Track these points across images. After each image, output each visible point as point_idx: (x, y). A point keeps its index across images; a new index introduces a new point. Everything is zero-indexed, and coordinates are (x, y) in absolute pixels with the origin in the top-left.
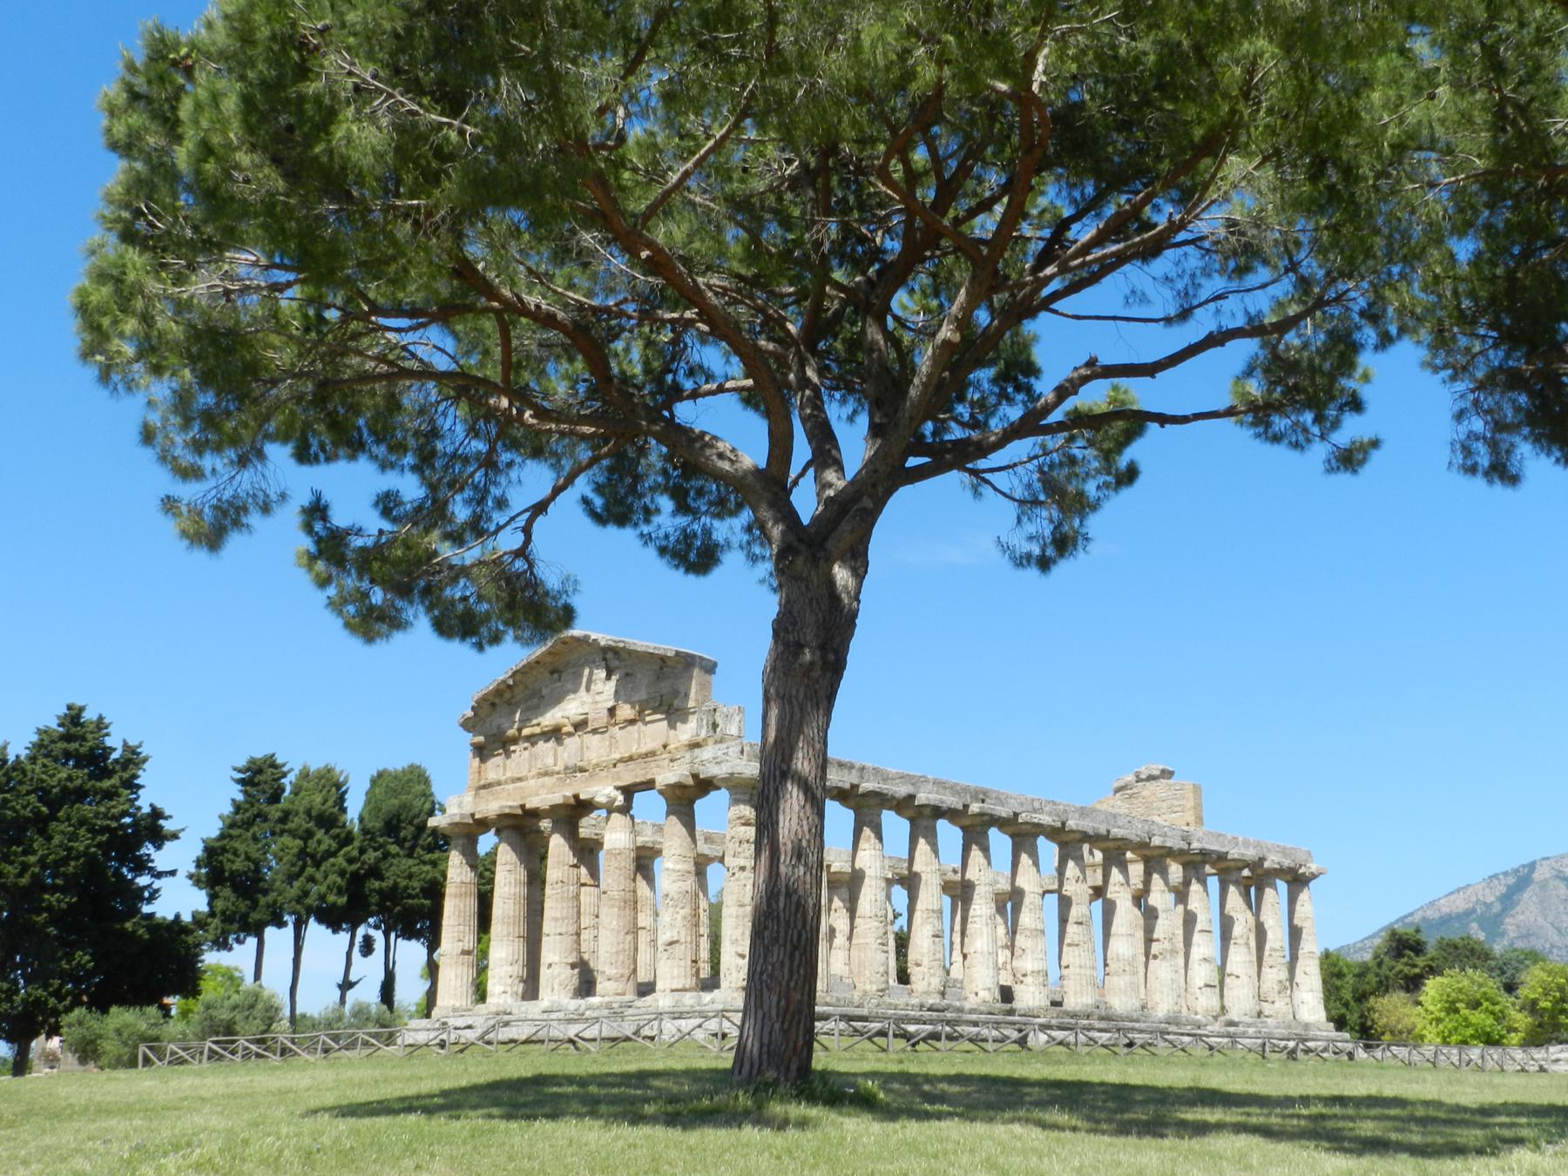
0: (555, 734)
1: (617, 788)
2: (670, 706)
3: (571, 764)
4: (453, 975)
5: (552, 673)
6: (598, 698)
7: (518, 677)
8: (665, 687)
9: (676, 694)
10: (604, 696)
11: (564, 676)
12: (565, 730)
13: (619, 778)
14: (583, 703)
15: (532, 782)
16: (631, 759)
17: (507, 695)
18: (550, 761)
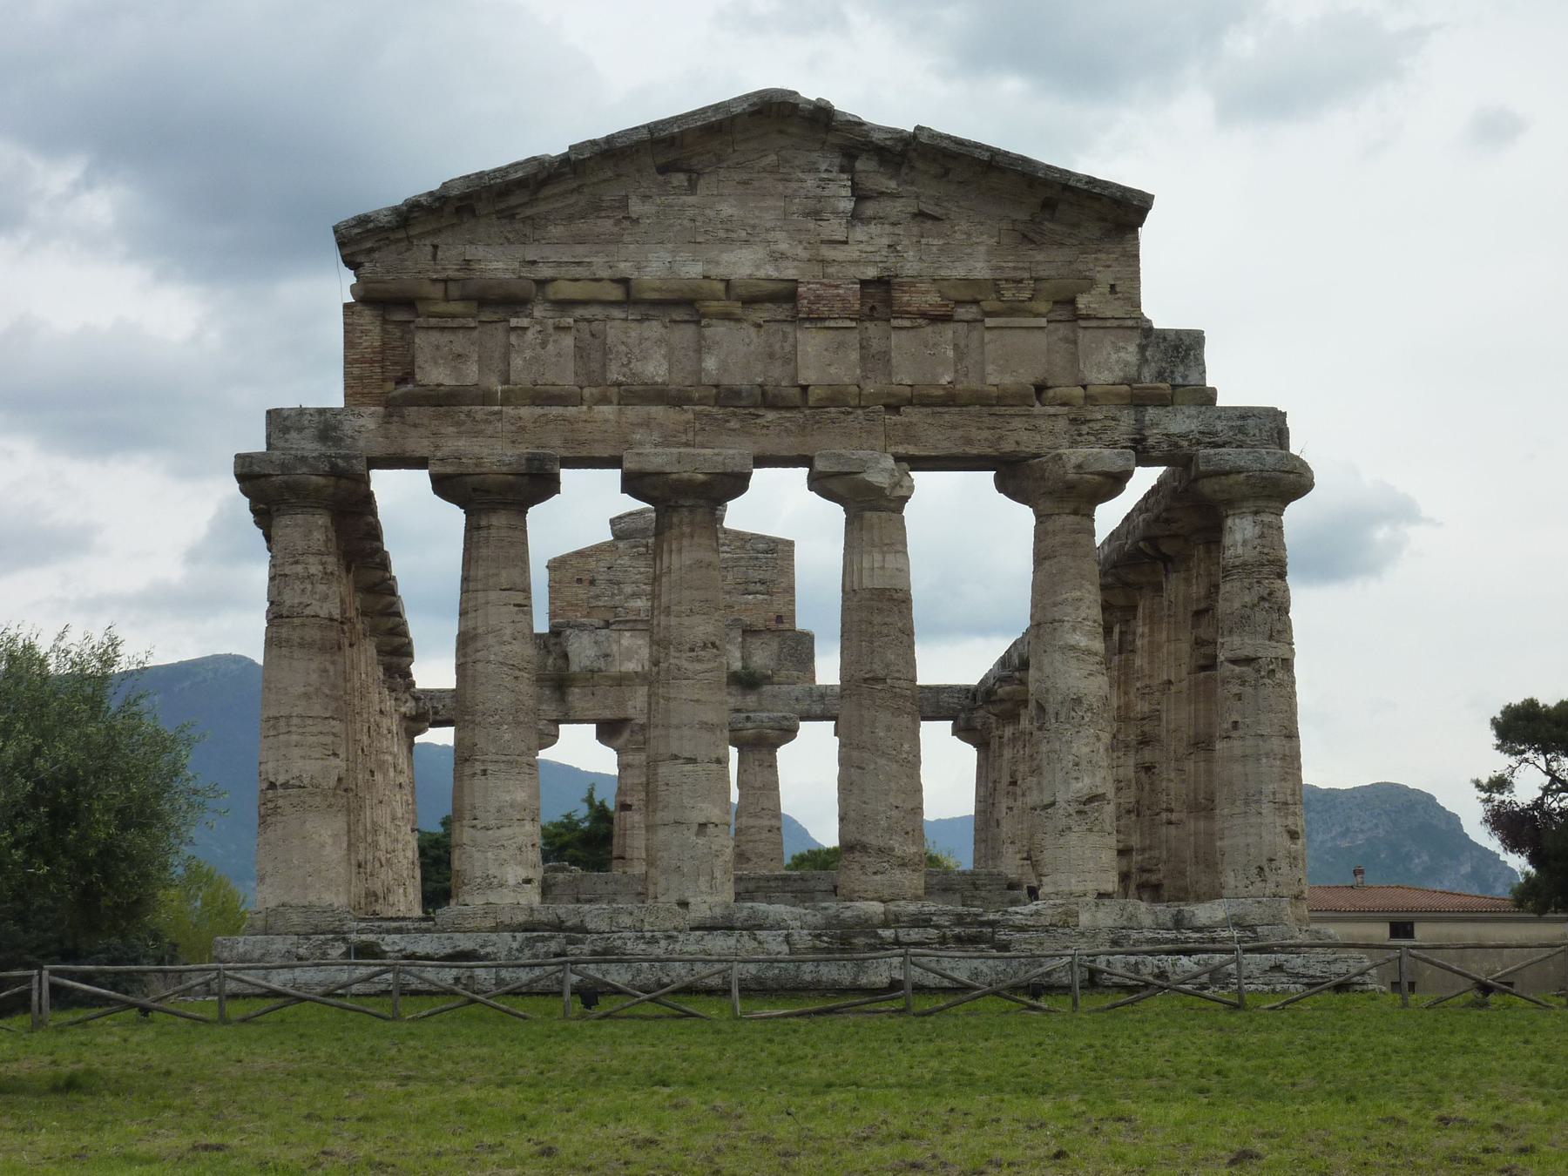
0: (685, 305)
1: (898, 459)
3: (737, 379)
4: (326, 836)
5: (664, 170)
6: (828, 252)
9: (1091, 283)
10: (852, 252)
12: (714, 306)
13: (910, 438)
14: (778, 257)
15: (607, 411)
16: (951, 399)
18: (655, 369)
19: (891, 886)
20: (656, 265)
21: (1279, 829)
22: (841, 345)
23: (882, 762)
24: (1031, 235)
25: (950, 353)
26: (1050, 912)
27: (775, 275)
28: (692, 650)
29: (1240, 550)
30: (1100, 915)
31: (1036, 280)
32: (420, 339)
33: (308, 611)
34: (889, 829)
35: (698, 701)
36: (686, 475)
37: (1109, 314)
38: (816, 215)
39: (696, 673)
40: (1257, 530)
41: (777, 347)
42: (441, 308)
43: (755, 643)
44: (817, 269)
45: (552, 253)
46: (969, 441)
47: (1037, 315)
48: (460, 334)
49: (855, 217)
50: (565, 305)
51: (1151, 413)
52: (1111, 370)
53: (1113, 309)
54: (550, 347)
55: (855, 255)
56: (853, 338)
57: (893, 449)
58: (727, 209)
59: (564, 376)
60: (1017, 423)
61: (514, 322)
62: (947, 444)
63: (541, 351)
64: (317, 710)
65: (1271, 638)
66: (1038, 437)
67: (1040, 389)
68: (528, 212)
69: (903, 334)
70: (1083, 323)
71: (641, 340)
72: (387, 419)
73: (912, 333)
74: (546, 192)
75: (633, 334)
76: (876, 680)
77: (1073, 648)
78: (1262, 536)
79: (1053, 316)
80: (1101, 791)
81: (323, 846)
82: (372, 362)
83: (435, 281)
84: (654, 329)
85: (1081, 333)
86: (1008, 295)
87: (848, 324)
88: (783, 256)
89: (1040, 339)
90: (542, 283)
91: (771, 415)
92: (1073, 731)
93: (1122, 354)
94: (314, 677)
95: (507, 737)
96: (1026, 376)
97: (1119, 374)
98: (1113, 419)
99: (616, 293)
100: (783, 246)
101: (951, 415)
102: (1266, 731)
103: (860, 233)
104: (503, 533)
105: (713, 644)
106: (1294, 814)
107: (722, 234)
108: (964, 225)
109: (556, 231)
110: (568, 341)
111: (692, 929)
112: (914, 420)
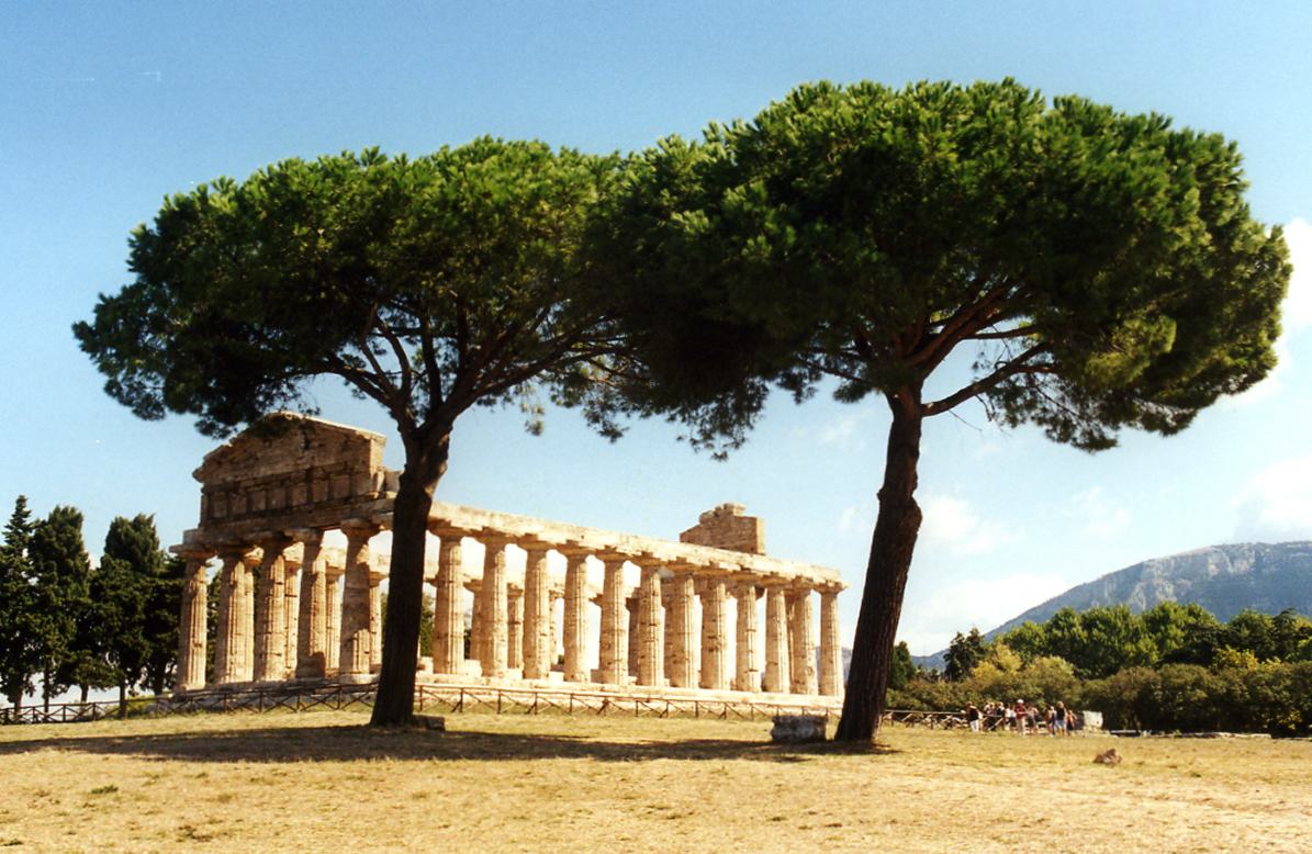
0: (267, 483)
2: (352, 469)
8: (348, 455)
11: (275, 444)
15: (249, 521)
18: (262, 506)
20: (264, 471)
49: (307, 448)
50: (246, 488)
56: (305, 489)
59: (243, 511)
63: (239, 506)
67: (346, 500)
96: (345, 493)
109: (242, 465)
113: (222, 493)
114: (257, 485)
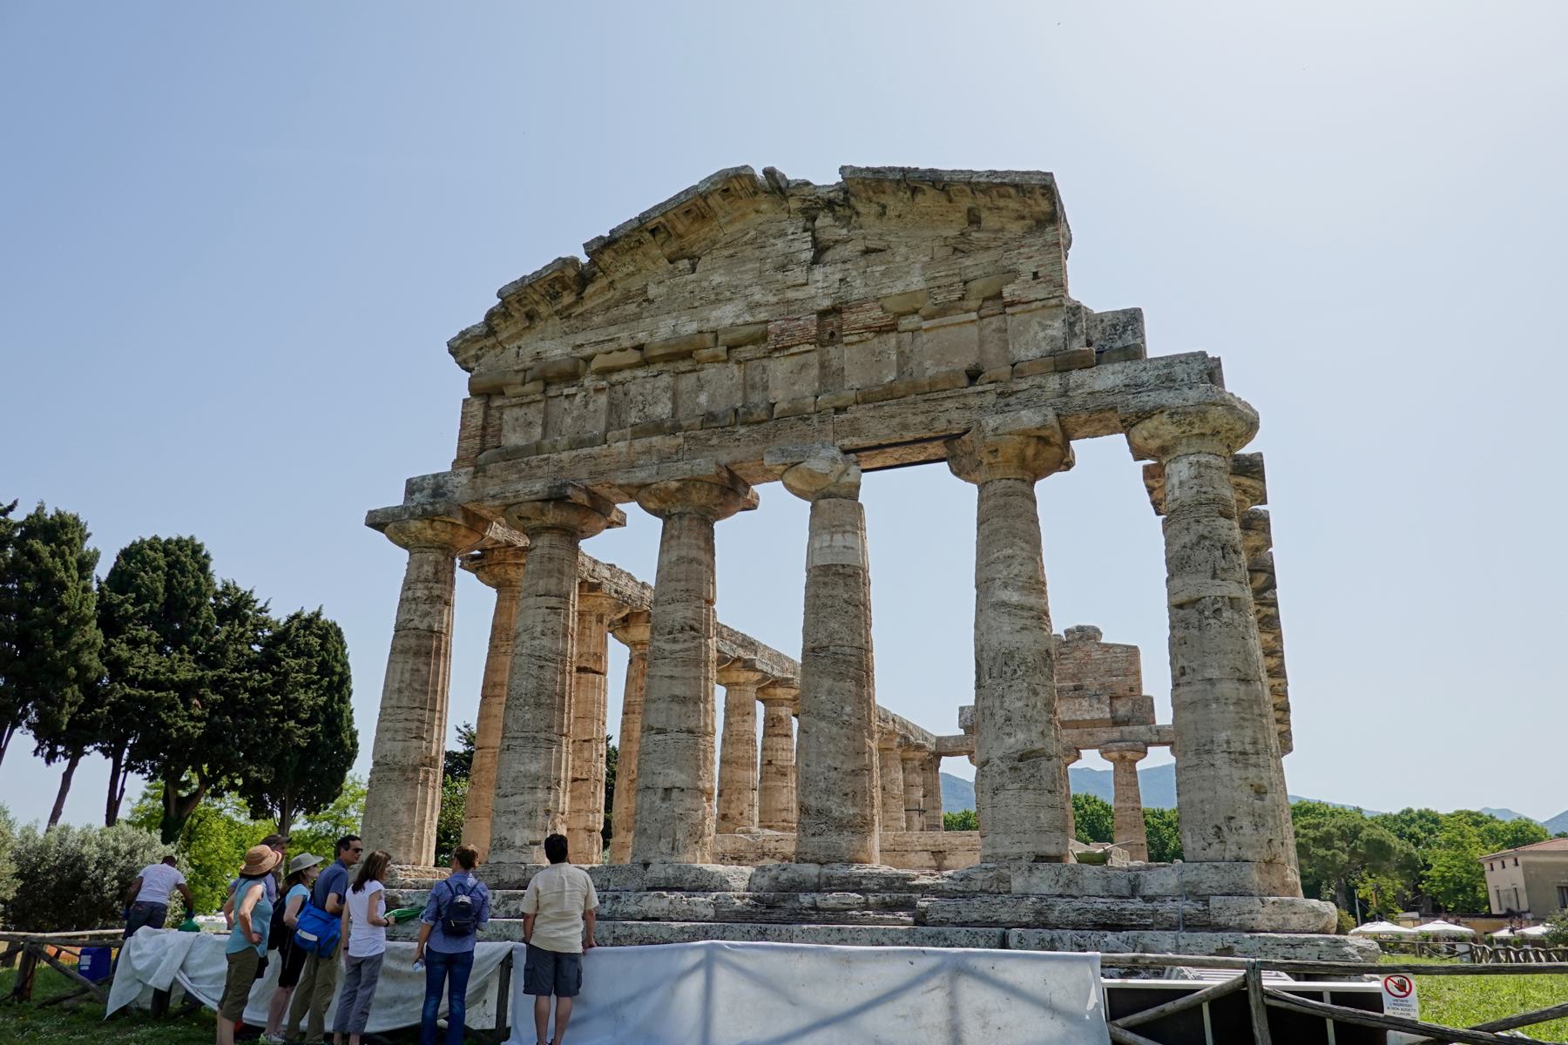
0: (681, 354)
3: (720, 407)
6: (791, 294)
7: (607, 257)
8: (976, 264)
9: (1012, 274)
13: (856, 431)
14: (753, 307)
16: (888, 394)
17: (568, 298)
18: (662, 410)
19: (827, 848)
20: (663, 329)
21: (1237, 782)
22: (804, 366)
23: (823, 724)
24: (961, 246)
25: (894, 358)
26: (980, 876)
27: (750, 319)
28: (670, 633)
29: (1177, 493)
30: (1034, 880)
31: (966, 283)
32: (508, 416)
33: (411, 625)
34: (828, 791)
35: (672, 677)
36: (662, 485)
37: (1032, 297)
38: (783, 268)
39: (672, 653)
40: (1193, 471)
41: (757, 379)
42: (520, 389)
43: (1117, 704)
44: (782, 309)
45: (592, 336)
46: (905, 427)
47: (968, 311)
48: (532, 407)
49: (816, 261)
50: (604, 372)
51: (1076, 376)
52: (1038, 347)
53: (1040, 291)
54: (591, 407)
55: (813, 292)
56: (814, 358)
57: (839, 443)
58: (717, 279)
59: (596, 426)
60: (948, 404)
61: (566, 391)
62: (887, 431)
63: (584, 409)
64: (405, 702)
65: (1214, 576)
66: (968, 414)
67: (973, 376)
68: (579, 310)
69: (854, 348)
70: (1008, 310)
71: (654, 388)
72: (475, 475)
73: (861, 346)
74: (590, 289)
75: (648, 386)
76: (822, 648)
77: (1004, 604)
78: (1199, 476)
79: (983, 312)
80: (1038, 746)
81: (396, 813)
82: (474, 437)
83: (517, 372)
84: (666, 379)
85: (1009, 318)
86: (940, 298)
87: (808, 347)
88: (758, 305)
89: (973, 330)
90: (588, 360)
91: (742, 430)
92: (1005, 686)
93: (1050, 332)
94: (407, 675)
95: (528, 716)
96: (965, 361)
97: (1045, 346)
98: (1040, 387)
99: (635, 357)
100: (757, 297)
101: (889, 408)
102: (1213, 673)
103: (818, 273)
104: (546, 551)
105: (692, 628)
106: (1256, 766)
107: (713, 297)
108: (903, 250)
109: (596, 320)
110: (603, 399)
111: (649, 889)
112: (858, 415)
113: (529, 387)
114: (646, 362)
